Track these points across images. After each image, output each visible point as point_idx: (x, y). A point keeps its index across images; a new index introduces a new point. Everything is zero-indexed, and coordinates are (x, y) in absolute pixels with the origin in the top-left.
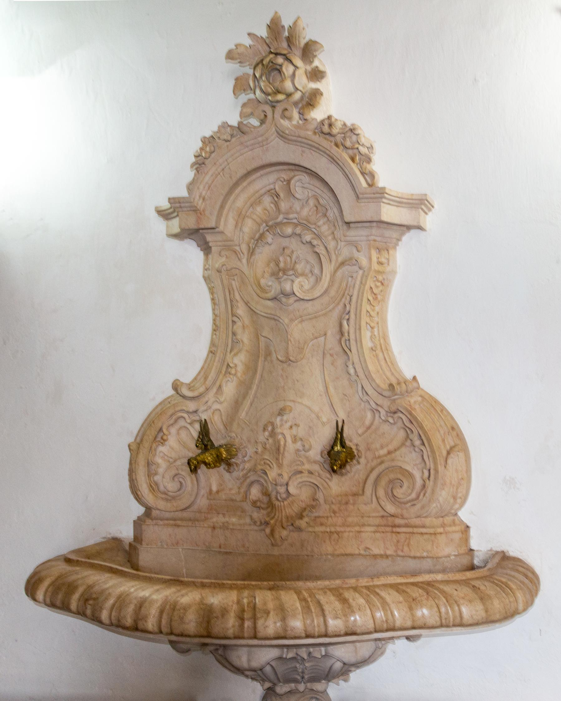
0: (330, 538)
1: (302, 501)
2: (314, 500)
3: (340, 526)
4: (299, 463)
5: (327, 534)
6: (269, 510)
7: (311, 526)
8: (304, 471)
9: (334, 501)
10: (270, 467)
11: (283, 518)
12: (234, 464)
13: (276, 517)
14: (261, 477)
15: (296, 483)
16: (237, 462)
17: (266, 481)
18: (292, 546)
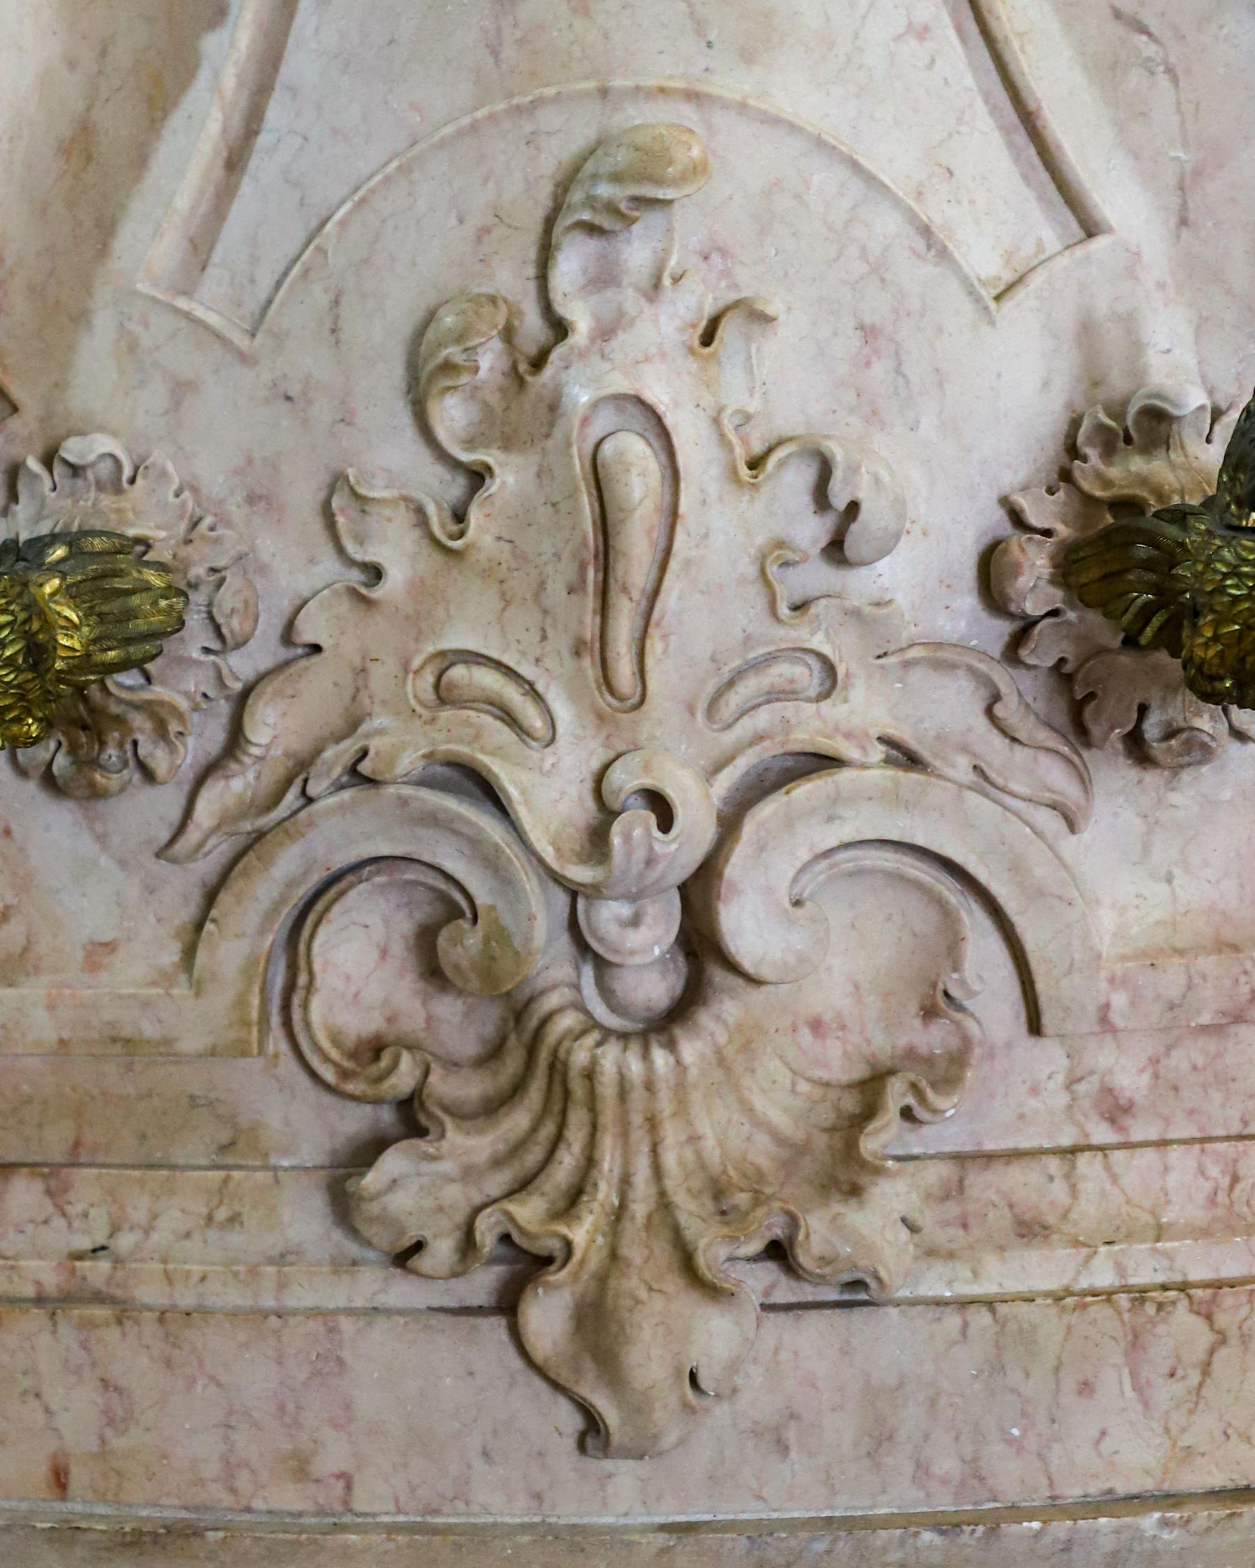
0: (1136, 1343)
1: (817, 1026)
2: (929, 1013)
3: (1203, 1233)
4: (782, 672)
5: (1099, 1312)
6: (518, 1120)
7: (931, 1253)
8: (848, 750)
9: (1119, 1000)
10: (510, 719)
11: (681, 1198)
12: (139, 721)
13: (605, 1192)
14: (434, 820)
15: (783, 868)
16: (158, 692)
17: (492, 863)
18: (783, 1448)
